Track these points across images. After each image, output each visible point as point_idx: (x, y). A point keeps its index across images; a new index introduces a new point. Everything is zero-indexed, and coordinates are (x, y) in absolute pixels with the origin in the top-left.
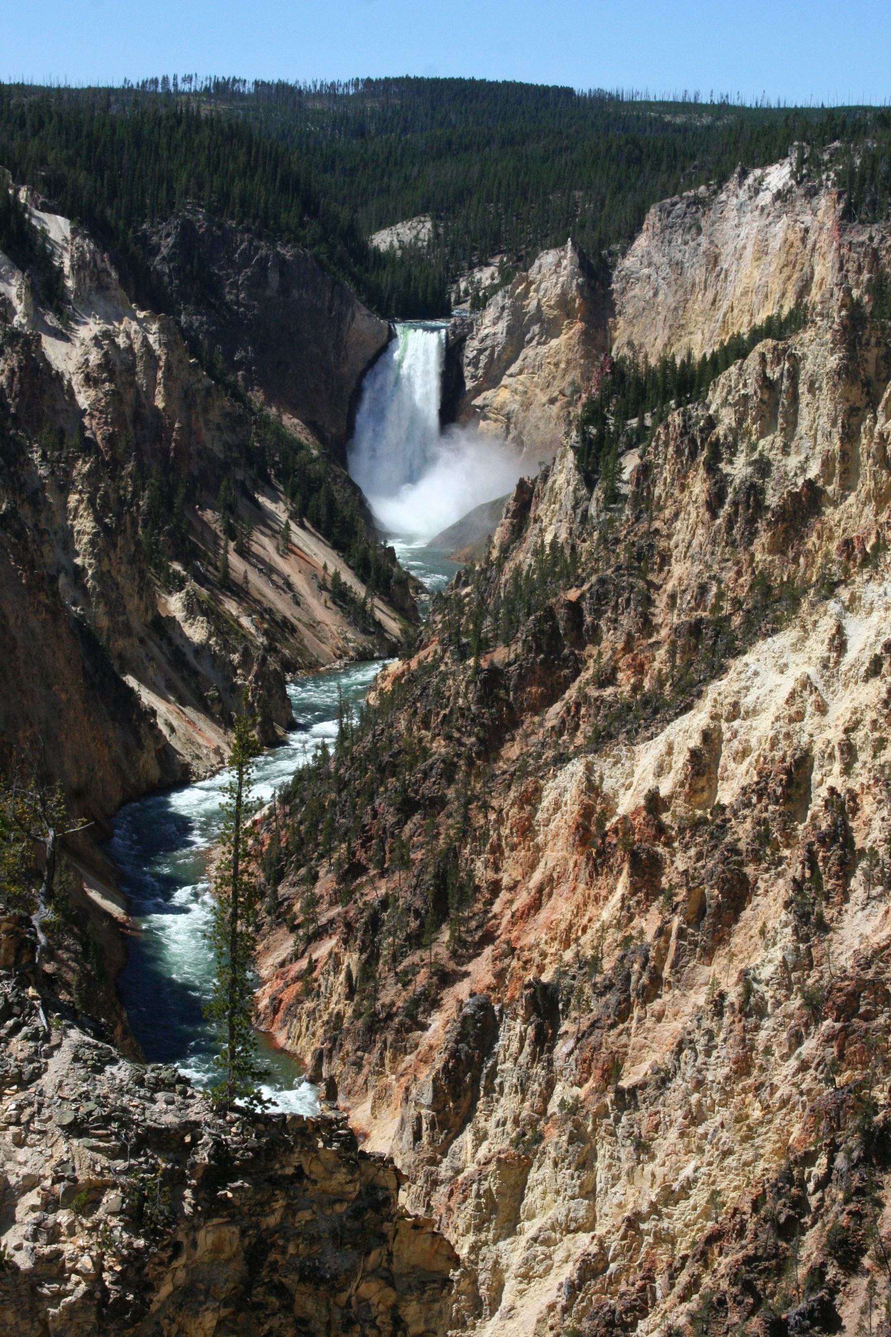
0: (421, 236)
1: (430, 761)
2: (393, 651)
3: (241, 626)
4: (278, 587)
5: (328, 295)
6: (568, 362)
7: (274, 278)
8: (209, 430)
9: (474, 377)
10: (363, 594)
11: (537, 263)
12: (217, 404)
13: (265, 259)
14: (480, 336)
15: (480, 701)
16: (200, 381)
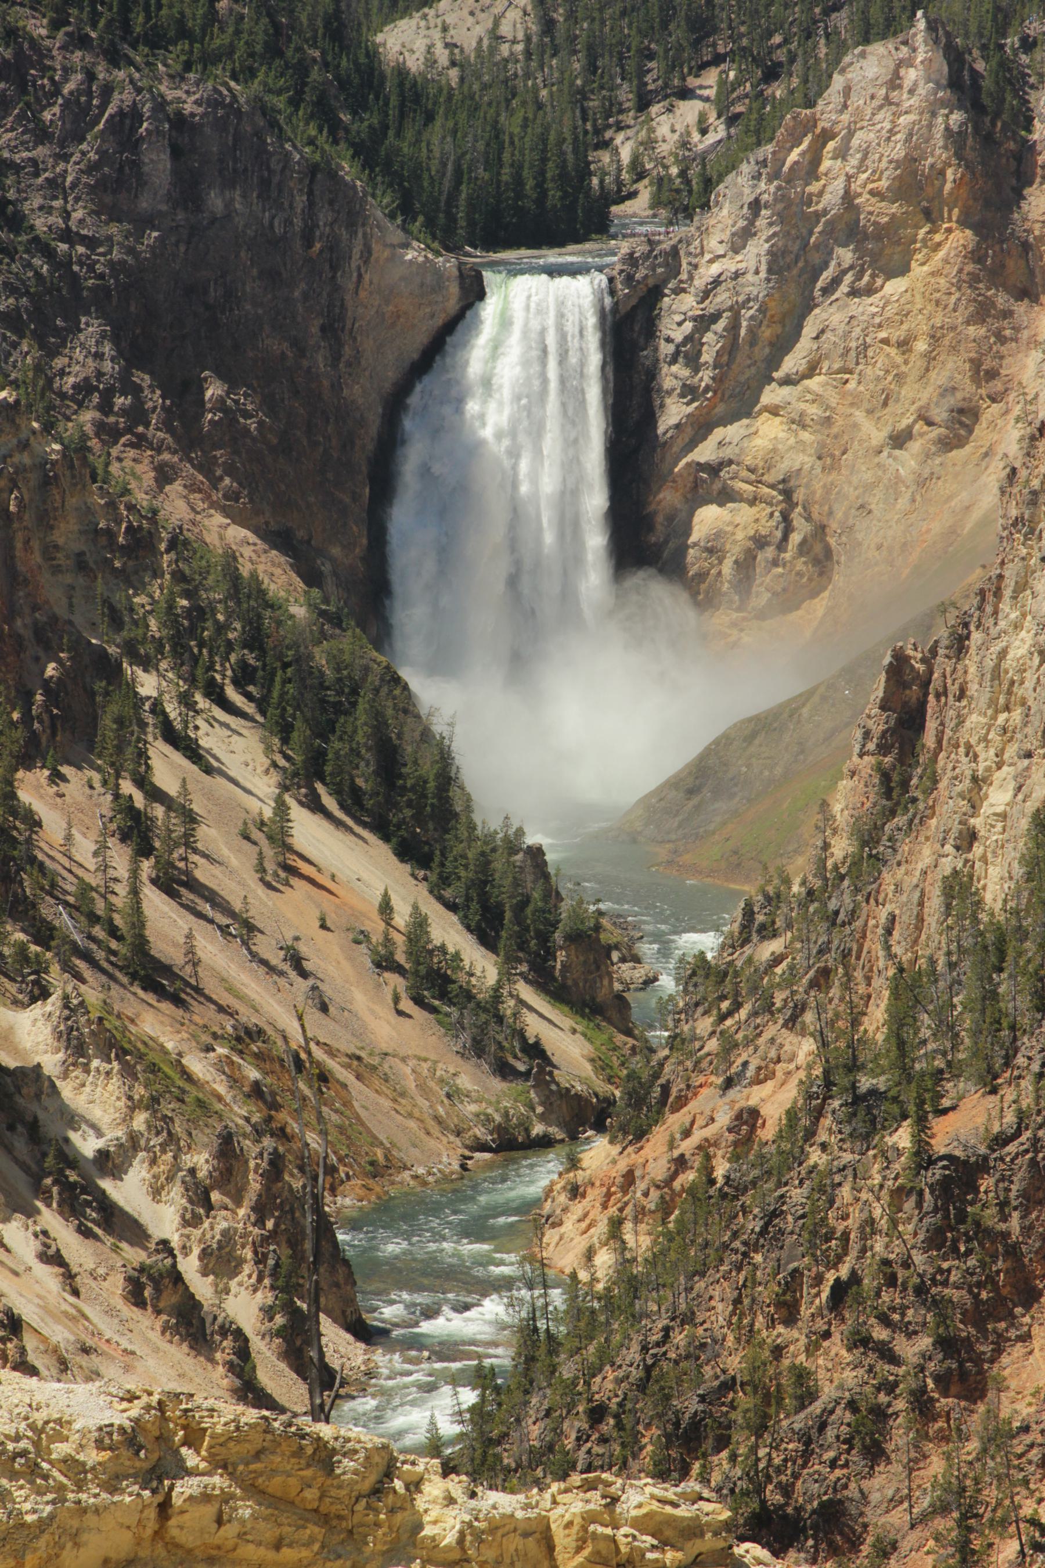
0: (505, 29)
1: (816, 1408)
2: (584, 1116)
3: (187, 1076)
4: (271, 969)
5: (301, 201)
6: (934, 338)
7: (157, 163)
8: (56, 570)
9: (689, 391)
10: (492, 976)
11: (838, 81)
12: (72, 502)
13: (131, 116)
14: (699, 283)
15: (935, 1240)
16: (24, 446)
